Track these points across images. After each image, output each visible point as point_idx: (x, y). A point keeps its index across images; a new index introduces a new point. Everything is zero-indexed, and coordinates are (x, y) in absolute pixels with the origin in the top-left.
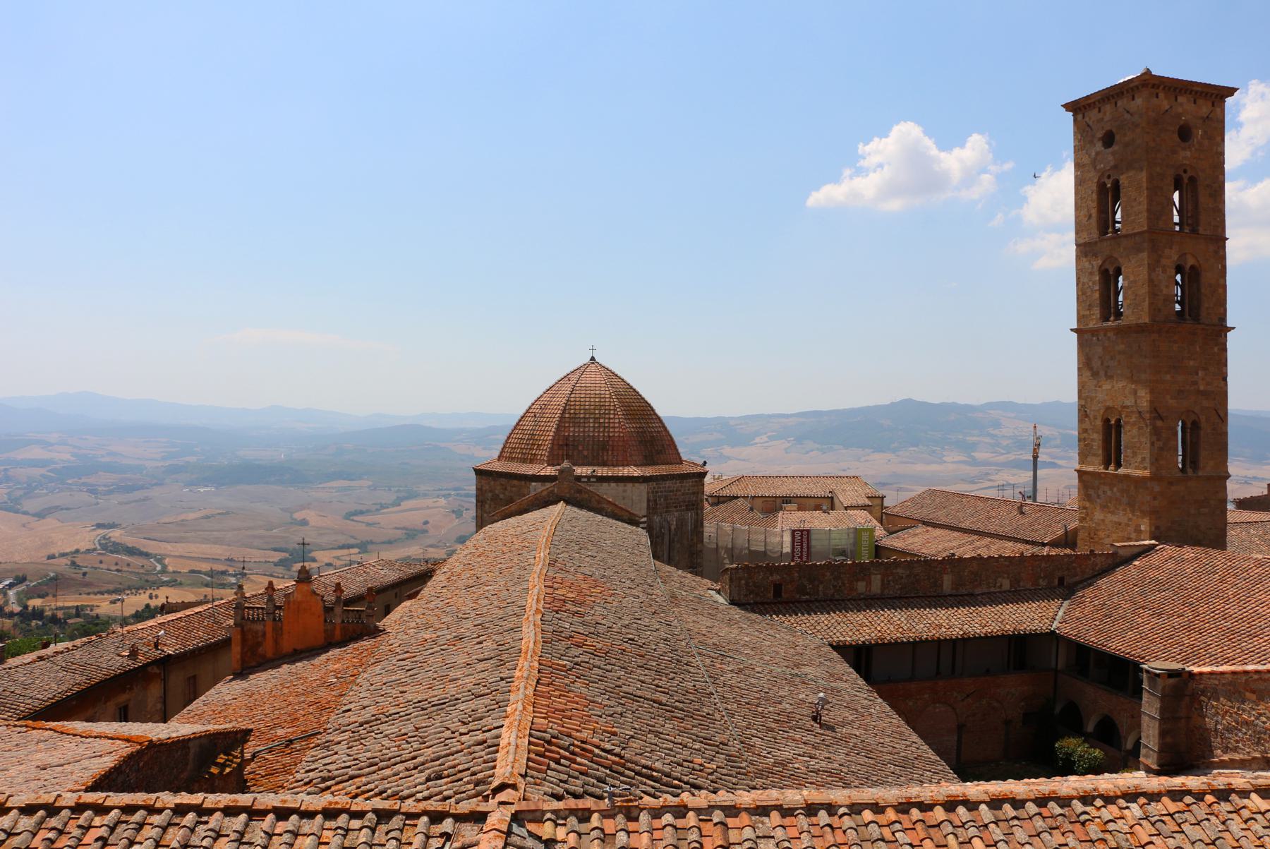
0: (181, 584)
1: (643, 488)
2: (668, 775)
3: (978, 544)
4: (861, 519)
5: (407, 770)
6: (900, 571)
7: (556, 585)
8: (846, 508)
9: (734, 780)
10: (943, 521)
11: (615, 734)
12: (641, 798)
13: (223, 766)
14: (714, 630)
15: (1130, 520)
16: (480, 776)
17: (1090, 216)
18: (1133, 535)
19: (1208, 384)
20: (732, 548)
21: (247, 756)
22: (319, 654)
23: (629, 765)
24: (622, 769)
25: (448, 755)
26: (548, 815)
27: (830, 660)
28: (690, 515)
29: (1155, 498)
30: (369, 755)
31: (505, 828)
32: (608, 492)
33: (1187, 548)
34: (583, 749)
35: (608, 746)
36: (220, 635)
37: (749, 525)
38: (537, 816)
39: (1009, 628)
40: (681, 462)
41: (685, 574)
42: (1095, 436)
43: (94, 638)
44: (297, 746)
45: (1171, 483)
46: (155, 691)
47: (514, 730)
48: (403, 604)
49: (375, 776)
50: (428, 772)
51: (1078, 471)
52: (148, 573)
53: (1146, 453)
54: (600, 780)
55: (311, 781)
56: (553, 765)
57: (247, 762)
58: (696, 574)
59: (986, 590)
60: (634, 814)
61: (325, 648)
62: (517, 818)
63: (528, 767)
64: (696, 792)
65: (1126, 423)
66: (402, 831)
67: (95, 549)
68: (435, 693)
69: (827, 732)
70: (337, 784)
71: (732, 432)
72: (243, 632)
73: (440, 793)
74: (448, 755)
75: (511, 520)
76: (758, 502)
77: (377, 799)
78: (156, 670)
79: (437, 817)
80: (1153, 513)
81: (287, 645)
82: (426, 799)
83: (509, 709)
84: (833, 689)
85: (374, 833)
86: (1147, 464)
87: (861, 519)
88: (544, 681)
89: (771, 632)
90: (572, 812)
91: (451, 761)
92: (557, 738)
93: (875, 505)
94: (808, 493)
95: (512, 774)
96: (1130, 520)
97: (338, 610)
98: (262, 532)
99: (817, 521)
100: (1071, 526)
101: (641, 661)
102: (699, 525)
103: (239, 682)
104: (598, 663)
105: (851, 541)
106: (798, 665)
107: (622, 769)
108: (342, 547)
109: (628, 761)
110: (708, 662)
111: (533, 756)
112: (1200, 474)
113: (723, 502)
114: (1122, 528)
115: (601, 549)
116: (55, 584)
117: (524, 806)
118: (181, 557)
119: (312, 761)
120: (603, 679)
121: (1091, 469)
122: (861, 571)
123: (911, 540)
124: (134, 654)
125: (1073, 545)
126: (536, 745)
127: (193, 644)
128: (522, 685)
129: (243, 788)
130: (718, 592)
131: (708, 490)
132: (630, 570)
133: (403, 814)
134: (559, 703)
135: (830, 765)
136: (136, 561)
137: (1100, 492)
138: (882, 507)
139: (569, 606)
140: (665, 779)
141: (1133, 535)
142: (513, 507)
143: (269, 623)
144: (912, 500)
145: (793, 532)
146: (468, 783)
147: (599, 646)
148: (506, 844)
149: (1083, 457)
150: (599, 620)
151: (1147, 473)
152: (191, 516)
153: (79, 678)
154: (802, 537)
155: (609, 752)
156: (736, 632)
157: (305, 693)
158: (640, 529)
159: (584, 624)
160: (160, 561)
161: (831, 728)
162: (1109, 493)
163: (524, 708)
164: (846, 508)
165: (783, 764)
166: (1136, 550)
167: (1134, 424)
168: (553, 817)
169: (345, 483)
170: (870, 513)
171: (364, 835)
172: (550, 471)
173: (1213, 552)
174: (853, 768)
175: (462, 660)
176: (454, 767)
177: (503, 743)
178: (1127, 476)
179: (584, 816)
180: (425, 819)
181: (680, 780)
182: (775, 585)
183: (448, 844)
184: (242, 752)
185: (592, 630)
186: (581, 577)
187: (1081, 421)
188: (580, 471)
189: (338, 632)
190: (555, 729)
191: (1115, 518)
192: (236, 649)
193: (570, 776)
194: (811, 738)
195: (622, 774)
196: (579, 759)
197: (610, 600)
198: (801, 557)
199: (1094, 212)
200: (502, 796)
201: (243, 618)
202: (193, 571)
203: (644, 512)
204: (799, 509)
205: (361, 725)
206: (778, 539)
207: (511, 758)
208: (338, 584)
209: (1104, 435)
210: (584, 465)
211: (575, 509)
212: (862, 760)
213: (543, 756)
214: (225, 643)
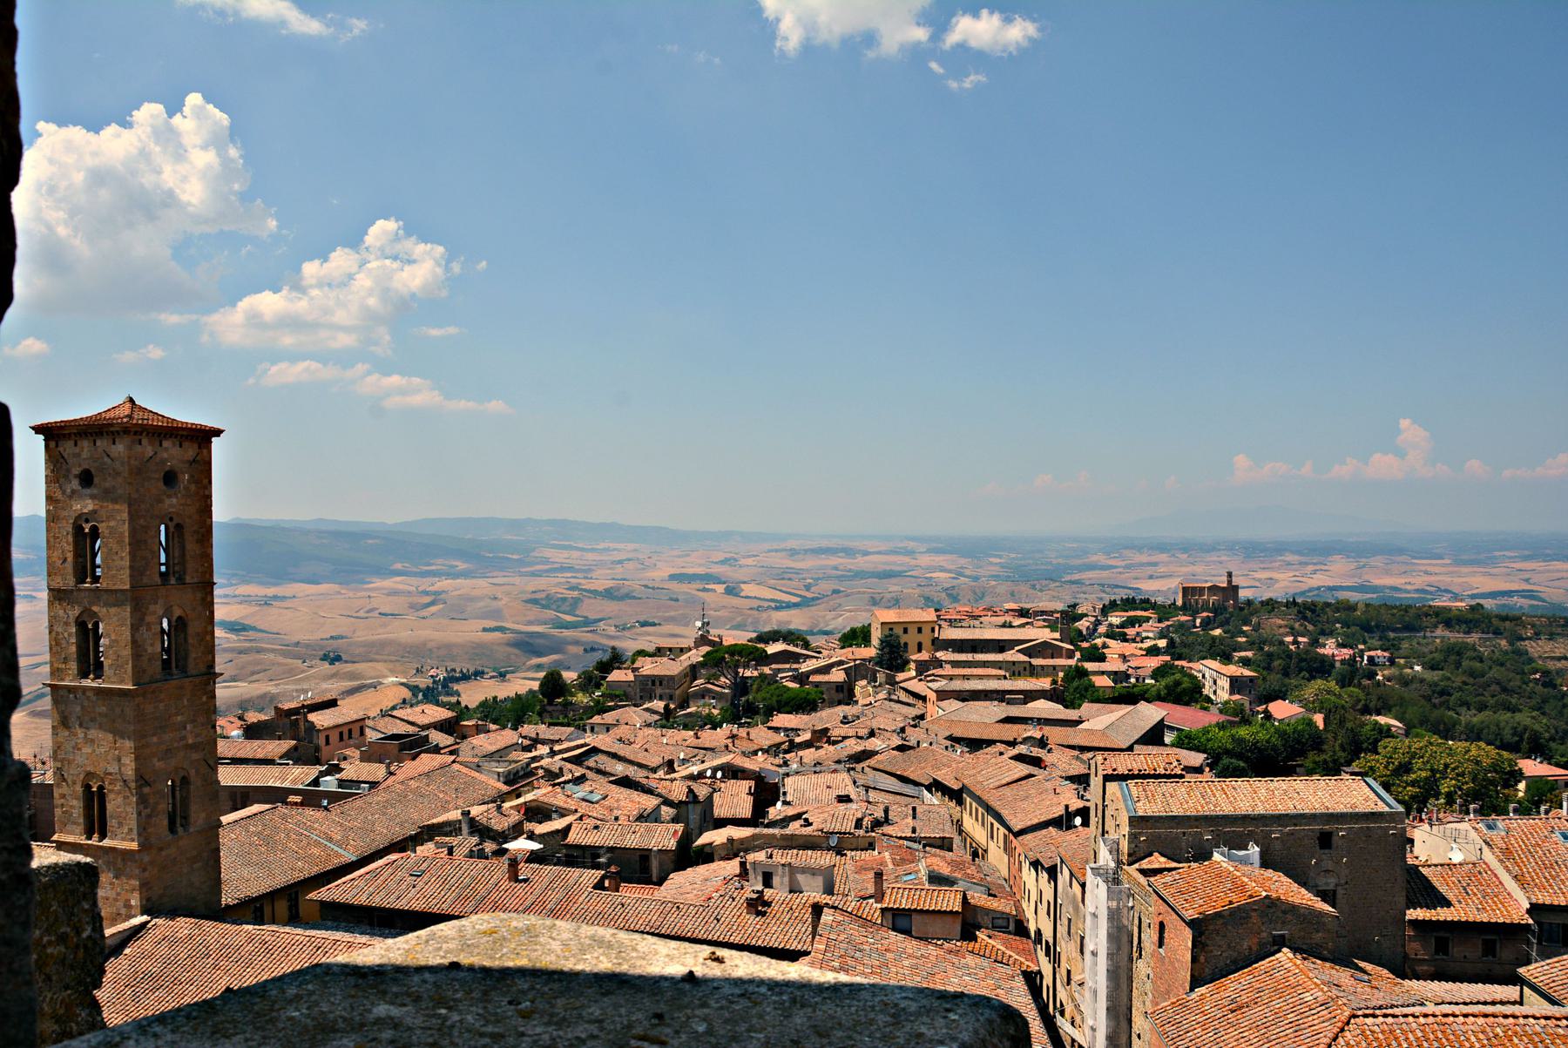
17: (65, 560)
19: (197, 735)
45: (161, 849)
53: (133, 824)
151: (134, 846)
167: (119, 793)
199: (70, 556)
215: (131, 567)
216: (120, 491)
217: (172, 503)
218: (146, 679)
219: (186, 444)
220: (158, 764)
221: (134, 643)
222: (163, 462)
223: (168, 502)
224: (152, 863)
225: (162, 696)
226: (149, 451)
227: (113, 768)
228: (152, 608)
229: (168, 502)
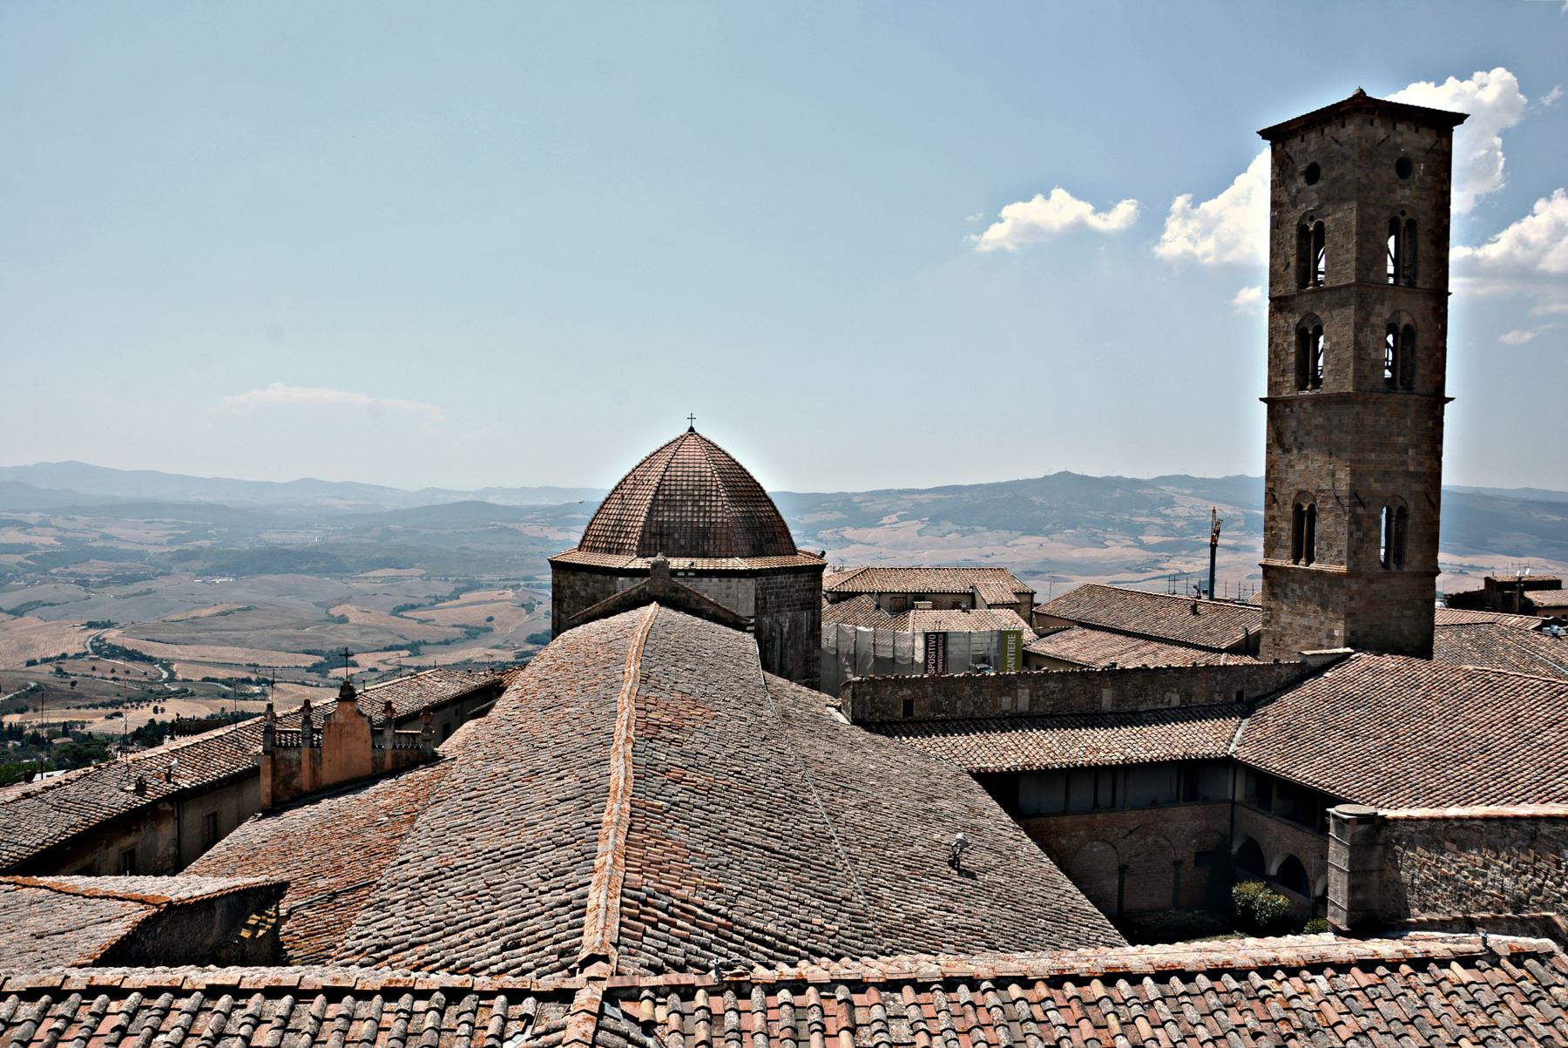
0: (192, 695)
2: (783, 939)
3: (1144, 650)
4: (1009, 619)
5: (478, 936)
6: (1051, 684)
7: (649, 707)
8: (989, 607)
9: (860, 944)
10: (1104, 621)
11: (720, 890)
12: (752, 968)
13: (256, 928)
14: (834, 757)
15: (1322, 623)
16: (565, 944)
18: (1325, 642)
21: (283, 912)
22: (366, 787)
23: (738, 927)
24: (729, 933)
25: (525, 919)
26: (646, 993)
27: (970, 791)
28: (805, 616)
29: (1351, 599)
30: (432, 917)
31: (595, 1009)
32: (709, 590)
33: (1388, 657)
34: (684, 910)
35: (713, 906)
36: (246, 764)
37: (875, 626)
38: (633, 994)
39: (1178, 752)
40: (795, 552)
41: (799, 688)
42: (1284, 525)
43: (91, 769)
44: (342, 900)
45: (1371, 581)
46: (167, 831)
47: (604, 888)
48: (466, 725)
49: (440, 944)
50: (503, 939)
51: (1263, 566)
52: (152, 681)
53: (1344, 545)
54: (704, 946)
55: (364, 949)
56: (649, 930)
57: (281, 920)
58: (812, 686)
59: (1151, 707)
60: (746, 989)
61: (373, 779)
62: (611, 996)
63: (621, 934)
64: (816, 960)
65: (1322, 510)
66: (475, 1012)
67: (86, 654)
68: (509, 841)
69: (967, 880)
70: (395, 952)
71: (854, 511)
72: (273, 759)
73: (519, 965)
74: (525, 919)
75: (594, 624)
76: (886, 600)
77: (443, 973)
78: (168, 807)
79: (515, 996)
80: (1350, 616)
81: (328, 775)
82: (501, 972)
83: (596, 862)
84: (973, 827)
85: (442, 1016)
86: (1344, 558)
87: (1009, 619)
88: (638, 826)
89: (900, 758)
90: (674, 988)
91: (531, 924)
92: (653, 897)
93: (1024, 603)
94: (944, 588)
95: (602, 943)
96: (1322, 623)
97: (388, 734)
98: (291, 631)
99: (955, 622)
100: (1252, 630)
101: (749, 799)
102: (816, 626)
103: (269, 820)
104: (699, 803)
106: (931, 799)
107: (729, 933)
108: (390, 649)
109: (736, 923)
110: (826, 796)
111: (626, 919)
112: (1405, 569)
114: (1313, 631)
115: (701, 661)
116: (37, 696)
117: (617, 982)
118: (192, 662)
119: (364, 925)
120: (705, 822)
121: (1278, 563)
122: (1006, 684)
123: (1065, 645)
124: (141, 788)
126: (630, 906)
127: (211, 776)
128: (611, 833)
129: (278, 958)
130: (839, 709)
131: (827, 584)
132: (736, 686)
133: (476, 993)
134: (655, 854)
135: (970, 921)
136: (138, 667)
137: (1288, 591)
138: (1032, 604)
139: (664, 733)
140: (779, 944)
141: (1325, 642)
142: (597, 608)
143: (306, 751)
144: (1067, 597)
145: (927, 635)
146: (551, 953)
147: (700, 781)
148: (598, 1028)
149: (1269, 549)
150: (700, 748)
151: (1343, 569)
152: (205, 612)
153: (75, 819)
154: (937, 641)
155: (715, 912)
156: (859, 758)
157: (350, 835)
159: (682, 754)
160: (166, 667)
161: (972, 876)
162: (1298, 592)
163: (615, 862)
164: (989, 607)
165: (916, 920)
166: (1328, 659)
167: (1330, 512)
168: (652, 995)
169: (393, 572)
170: (1018, 612)
171: (430, 1019)
172: (640, 563)
173: (1417, 662)
174: (997, 924)
175: (539, 799)
176: (533, 933)
177: (591, 904)
178: (1320, 573)
179: (687, 993)
180: (502, 998)
181: (796, 945)
182: (906, 702)
183: (530, 1028)
184: (277, 910)
185: (692, 762)
186: (679, 696)
187: (1268, 507)
188: (677, 563)
189: (388, 759)
190: (651, 885)
191: (1305, 622)
192: (265, 782)
193: (670, 943)
194: (947, 887)
195: (730, 939)
196: (679, 922)
197: (712, 723)
198: (935, 665)
200: (591, 971)
201: (274, 744)
202: (207, 679)
203: (752, 613)
204: (934, 608)
205: (422, 880)
206: (909, 643)
207: (600, 924)
208: (389, 704)
209: (1295, 524)
211: (670, 611)
212: (1007, 914)
213: (638, 919)
214: (253, 773)
216: (1348, 177)
217: (1405, 195)
219: (1423, 130)
220: (1376, 486)
222: (1397, 147)
223: (1400, 192)
224: (1360, 593)
225: (1384, 410)
227: (1326, 485)
228: (1378, 308)
229: (1400, 192)
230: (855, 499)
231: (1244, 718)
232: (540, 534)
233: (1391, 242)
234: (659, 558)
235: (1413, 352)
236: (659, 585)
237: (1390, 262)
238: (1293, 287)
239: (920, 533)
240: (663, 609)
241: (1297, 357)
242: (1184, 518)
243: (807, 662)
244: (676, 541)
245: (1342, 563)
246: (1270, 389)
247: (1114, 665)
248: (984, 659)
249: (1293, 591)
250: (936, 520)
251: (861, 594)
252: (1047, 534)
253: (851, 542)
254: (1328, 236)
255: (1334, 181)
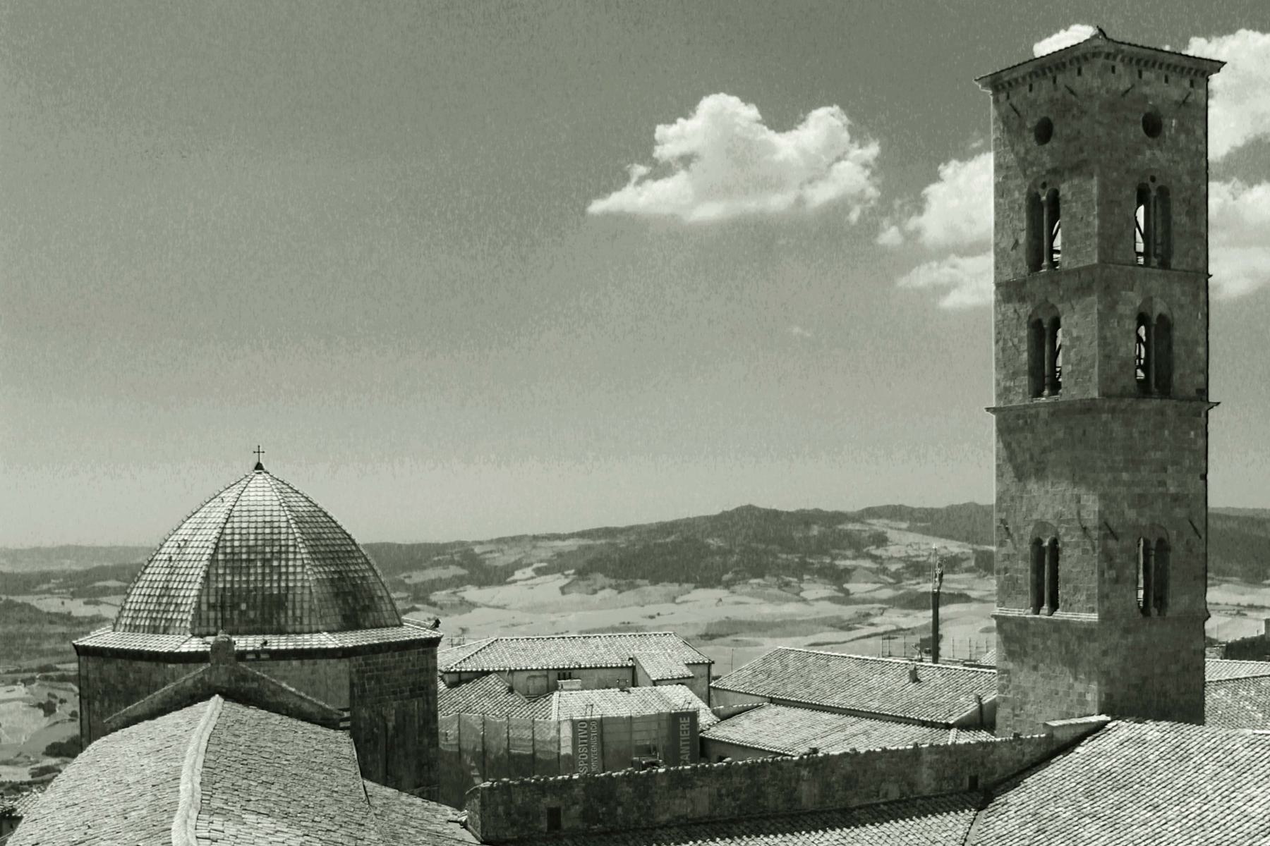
1: (343, 665)
4: (681, 698)
8: (655, 683)
20: (484, 752)
28: (415, 705)
33: (1151, 724)
58: (429, 797)
80: (1106, 677)
94: (597, 660)
100: (987, 700)
105: (665, 732)
112: (1168, 614)
113: (467, 681)
121: (1014, 612)
125: (990, 726)
130: (464, 825)
138: (709, 678)
151: (1094, 617)
158: (340, 733)
164: (655, 683)
166: (1081, 730)
167: (1077, 545)
188: (244, 643)
206: (553, 733)
210: (249, 633)
215: (1100, 235)
218: (1116, 388)
220: (1131, 514)
221: (1103, 342)
226: (1125, 84)
230: (477, 550)
231: (980, 809)
232: (63, 610)
233: (1141, 211)
234: (221, 636)
235: (1170, 347)
236: (221, 676)
237: (1139, 237)
238: (1023, 268)
239: (563, 590)
240: (227, 704)
241: (1030, 355)
242: (900, 559)
243: (420, 766)
244: (242, 613)
245: (1092, 610)
246: (999, 396)
247: (815, 751)
248: (649, 751)
249: (1034, 647)
250: (582, 573)
251: (488, 673)
252: (727, 585)
253: (473, 605)
254: (1063, 207)
255: (1069, 140)
